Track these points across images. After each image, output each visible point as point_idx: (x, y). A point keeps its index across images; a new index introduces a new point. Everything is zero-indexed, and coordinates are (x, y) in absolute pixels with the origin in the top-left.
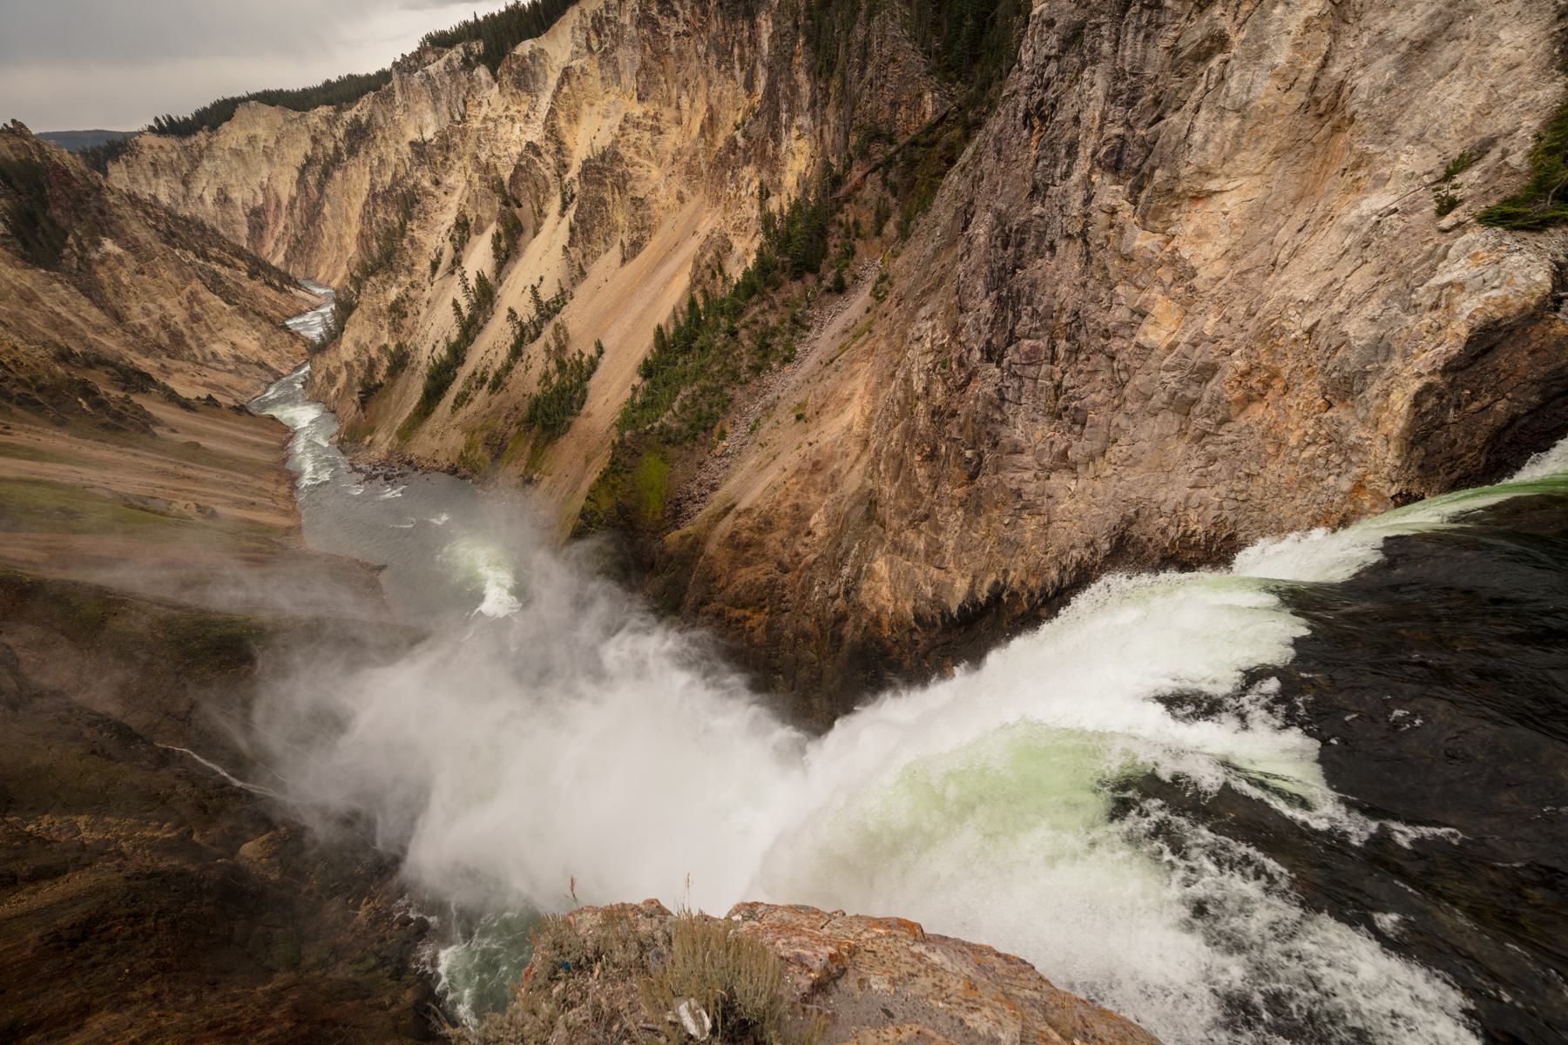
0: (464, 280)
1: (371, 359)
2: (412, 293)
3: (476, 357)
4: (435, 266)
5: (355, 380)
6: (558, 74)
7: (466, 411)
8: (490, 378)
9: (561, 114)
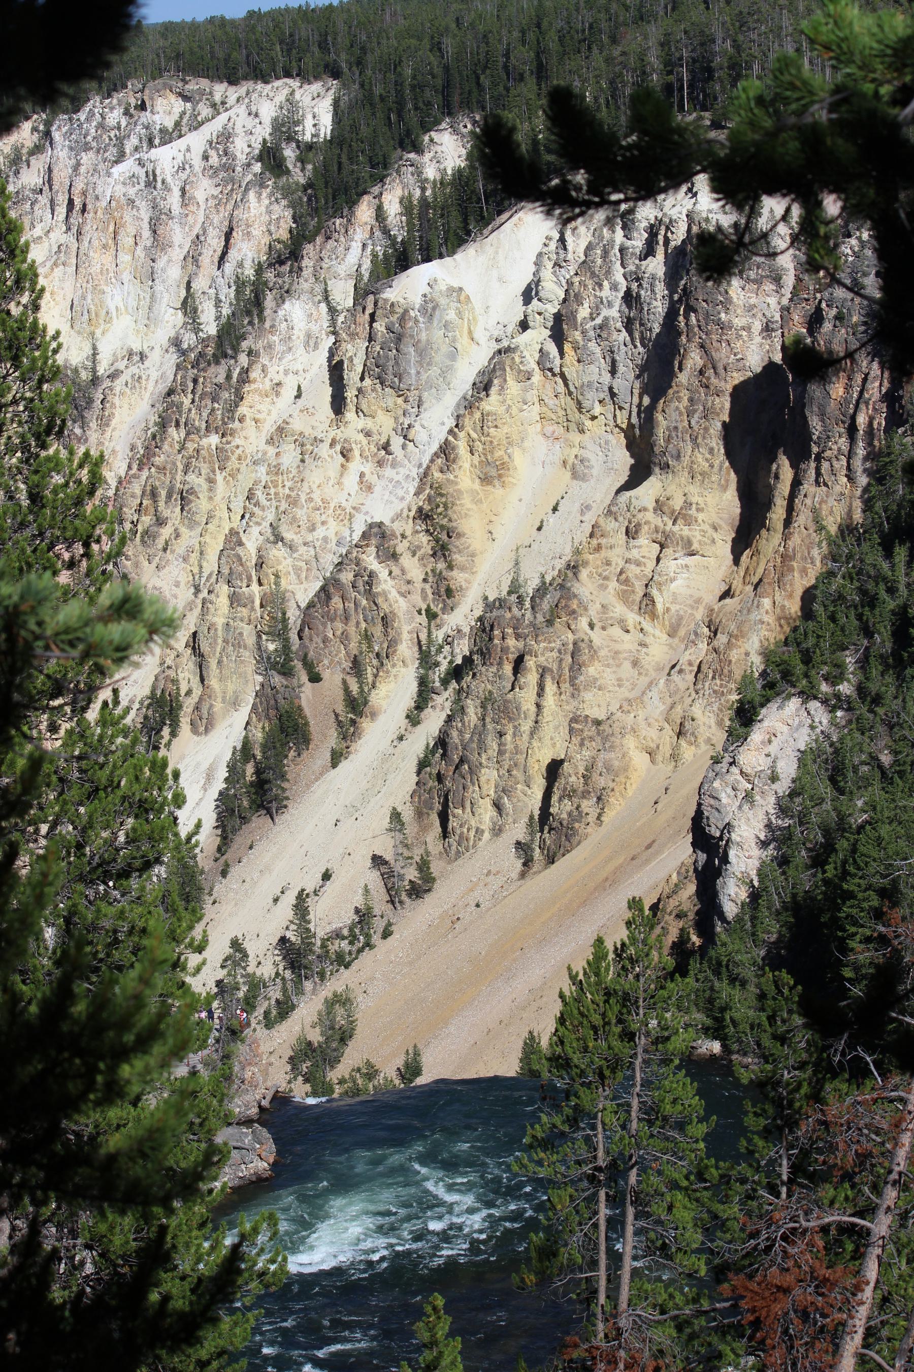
9: (465, 461)
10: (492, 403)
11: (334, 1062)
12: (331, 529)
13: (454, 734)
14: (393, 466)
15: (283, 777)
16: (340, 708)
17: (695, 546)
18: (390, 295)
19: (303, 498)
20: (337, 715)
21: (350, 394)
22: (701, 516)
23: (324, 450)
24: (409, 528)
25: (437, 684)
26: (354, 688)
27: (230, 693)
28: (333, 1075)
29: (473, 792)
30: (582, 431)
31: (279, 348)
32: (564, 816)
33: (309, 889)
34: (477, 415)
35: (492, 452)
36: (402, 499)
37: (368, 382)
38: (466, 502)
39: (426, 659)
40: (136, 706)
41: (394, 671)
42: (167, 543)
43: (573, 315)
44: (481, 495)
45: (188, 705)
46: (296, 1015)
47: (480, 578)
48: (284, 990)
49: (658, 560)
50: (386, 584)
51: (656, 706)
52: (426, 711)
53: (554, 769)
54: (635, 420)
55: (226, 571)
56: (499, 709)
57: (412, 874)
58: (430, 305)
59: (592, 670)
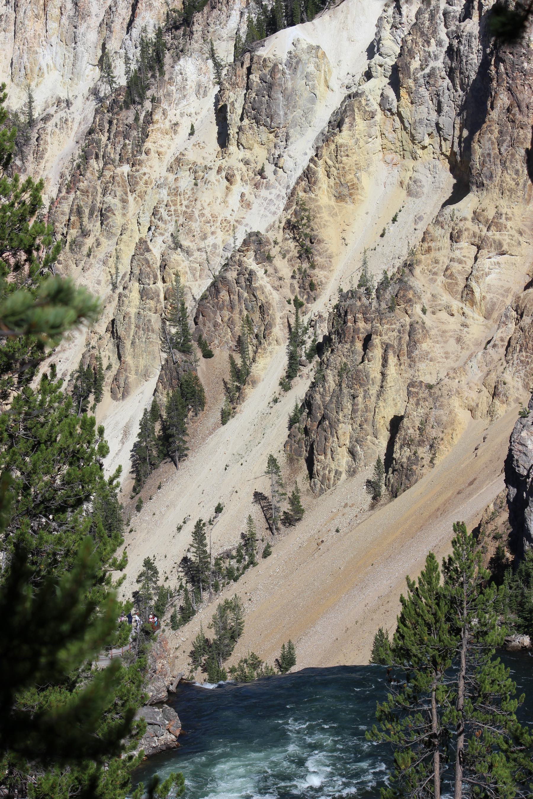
10: (344, 137)
11: (226, 655)
13: (318, 397)
14: (267, 187)
15: (184, 432)
16: (228, 377)
17: (505, 247)
18: (263, 52)
19: (197, 213)
20: (225, 383)
21: (232, 131)
22: (509, 224)
23: (212, 176)
24: (280, 236)
25: (304, 358)
26: (239, 361)
27: (141, 367)
28: (226, 666)
29: (333, 442)
30: (415, 158)
31: (176, 95)
32: (404, 460)
33: (205, 520)
34: (333, 147)
36: (275, 213)
37: (246, 122)
38: (325, 215)
39: (295, 339)
40: (68, 378)
41: (269, 348)
42: (90, 250)
43: (407, 66)
44: (337, 210)
45: (109, 376)
46: (196, 619)
48: (187, 599)
49: (476, 258)
50: (262, 281)
51: (475, 373)
52: (297, 379)
53: (396, 424)
54: (456, 149)
55: (137, 271)
56: (352, 377)
57: (285, 507)
58: (294, 61)
59: (425, 346)
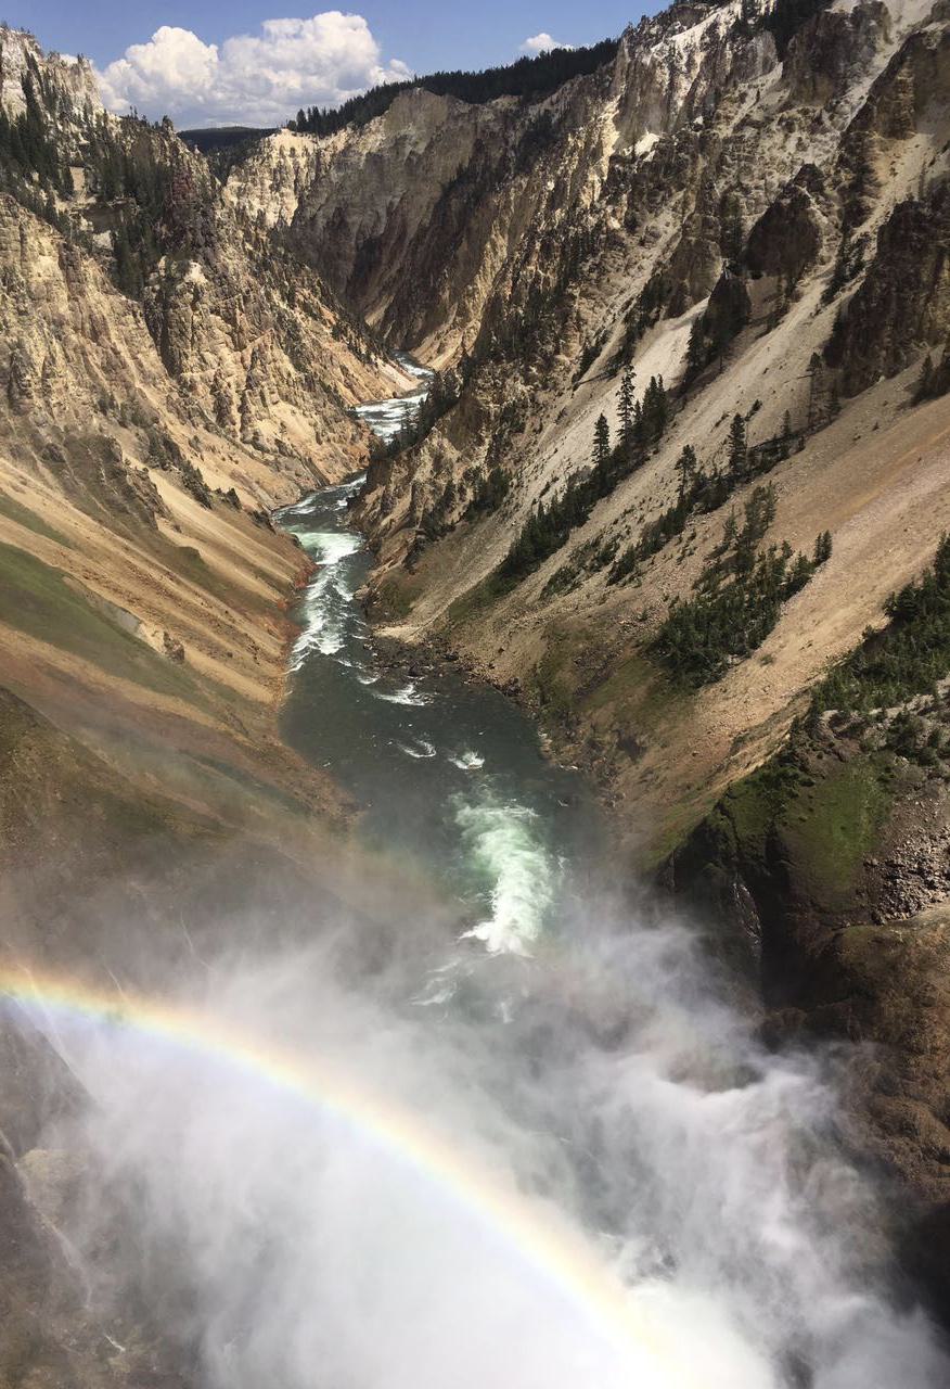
0: (628, 388)
1: (450, 485)
2: (542, 397)
3: (605, 516)
4: (589, 357)
5: (419, 514)
6: (894, 48)
7: (561, 603)
8: (619, 555)
12: (777, 178)
33: (744, 414)
35: (899, 111)
36: (828, 152)
38: (877, 150)
47: (884, 201)
